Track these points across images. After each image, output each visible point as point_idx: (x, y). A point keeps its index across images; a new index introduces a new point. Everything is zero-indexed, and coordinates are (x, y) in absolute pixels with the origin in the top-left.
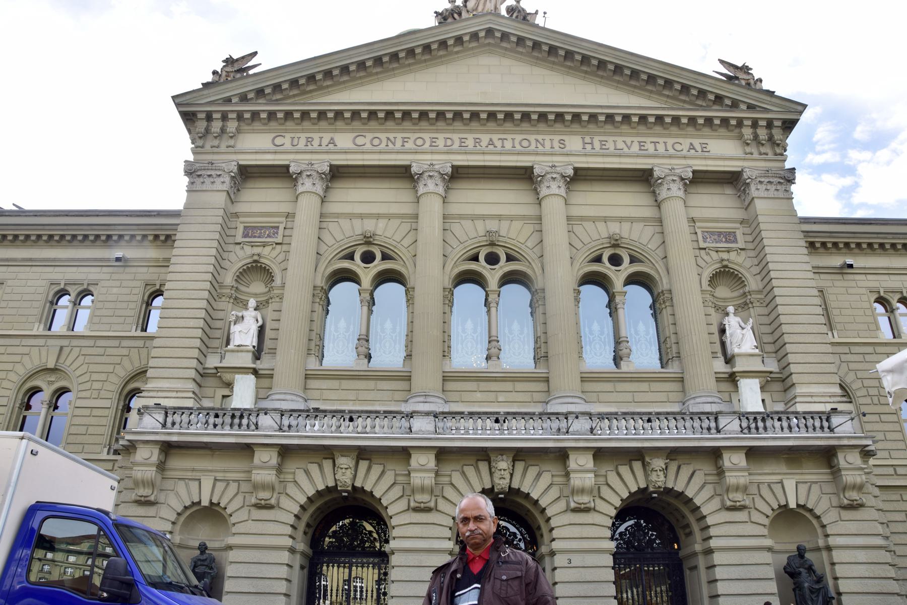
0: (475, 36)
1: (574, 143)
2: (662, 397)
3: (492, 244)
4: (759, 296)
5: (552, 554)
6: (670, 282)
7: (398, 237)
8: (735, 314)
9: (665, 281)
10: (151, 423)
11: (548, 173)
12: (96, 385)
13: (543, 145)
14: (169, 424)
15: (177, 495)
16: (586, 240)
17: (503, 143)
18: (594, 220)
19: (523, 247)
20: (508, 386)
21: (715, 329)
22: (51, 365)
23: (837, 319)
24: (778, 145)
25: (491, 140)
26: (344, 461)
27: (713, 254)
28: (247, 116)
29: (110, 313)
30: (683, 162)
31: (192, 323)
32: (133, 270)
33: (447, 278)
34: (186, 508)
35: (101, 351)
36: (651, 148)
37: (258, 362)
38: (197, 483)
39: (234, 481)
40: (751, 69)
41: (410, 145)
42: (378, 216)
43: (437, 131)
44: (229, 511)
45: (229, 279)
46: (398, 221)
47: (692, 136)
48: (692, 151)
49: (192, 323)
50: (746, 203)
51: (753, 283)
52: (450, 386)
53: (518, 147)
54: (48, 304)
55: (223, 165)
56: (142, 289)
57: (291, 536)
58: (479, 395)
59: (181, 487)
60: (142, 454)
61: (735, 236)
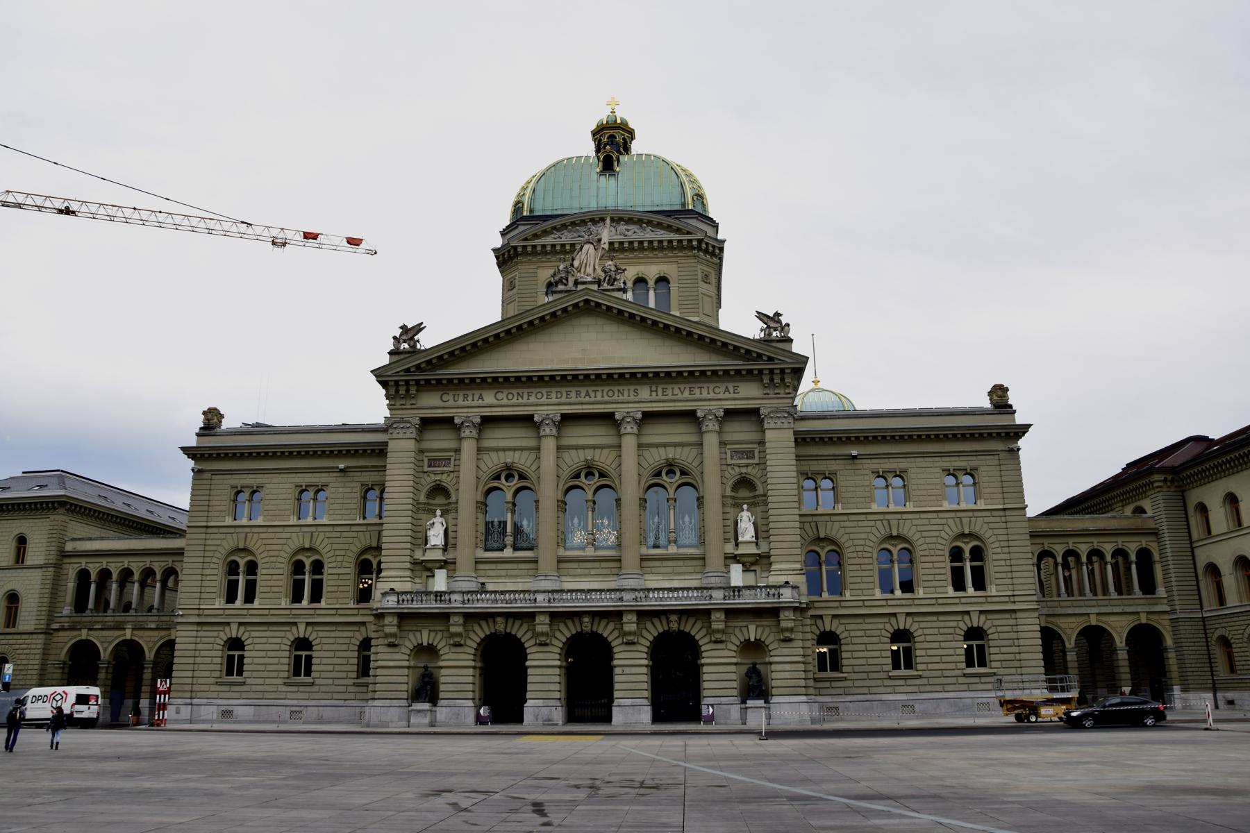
0: (576, 305)
1: (644, 392)
2: (690, 569)
3: (589, 467)
4: (764, 498)
5: (615, 666)
6: (703, 491)
7: (528, 464)
8: (747, 510)
9: (701, 489)
10: (391, 601)
11: (625, 417)
12: (339, 559)
13: (623, 394)
14: (401, 602)
15: (410, 640)
16: (651, 461)
17: (595, 394)
18: (657, 446)
19: (609, 468)
20: (597, 565)
21: (730, 523)
22: (307, 546)
23: (843, 495)
24: (788, 386)
25: (587, 391)
26: (499, 620)
27: (736, 468)
28: (422, 383)
29: (340, 506)
30: (719, 403)
31: (403, 533)
32: (351, 474)
33: (560, 492)
34: (415, 647)
35: (339, 534)
36: (697, 391)
37: (446, 553)
38: (419, 633)
39: (440, 631)
40: (780, 315)
41: (533, 399)
42: (514, 449)
43: (551, 387)
44: (438, 648)
45: (422, 498)
46: (527, 452)
47: (729, 381)
48: (727, 393)
49: (403, 533)
51: (760, 491)
52: (563, 565)
53: (606, 398)
54: (296, 501)
55: (410, 419)
56: (359, 488)
57: (474, 660)
58: (579, 570)
59: (411, 636)
60: (388, 620)
61: (754, 453)
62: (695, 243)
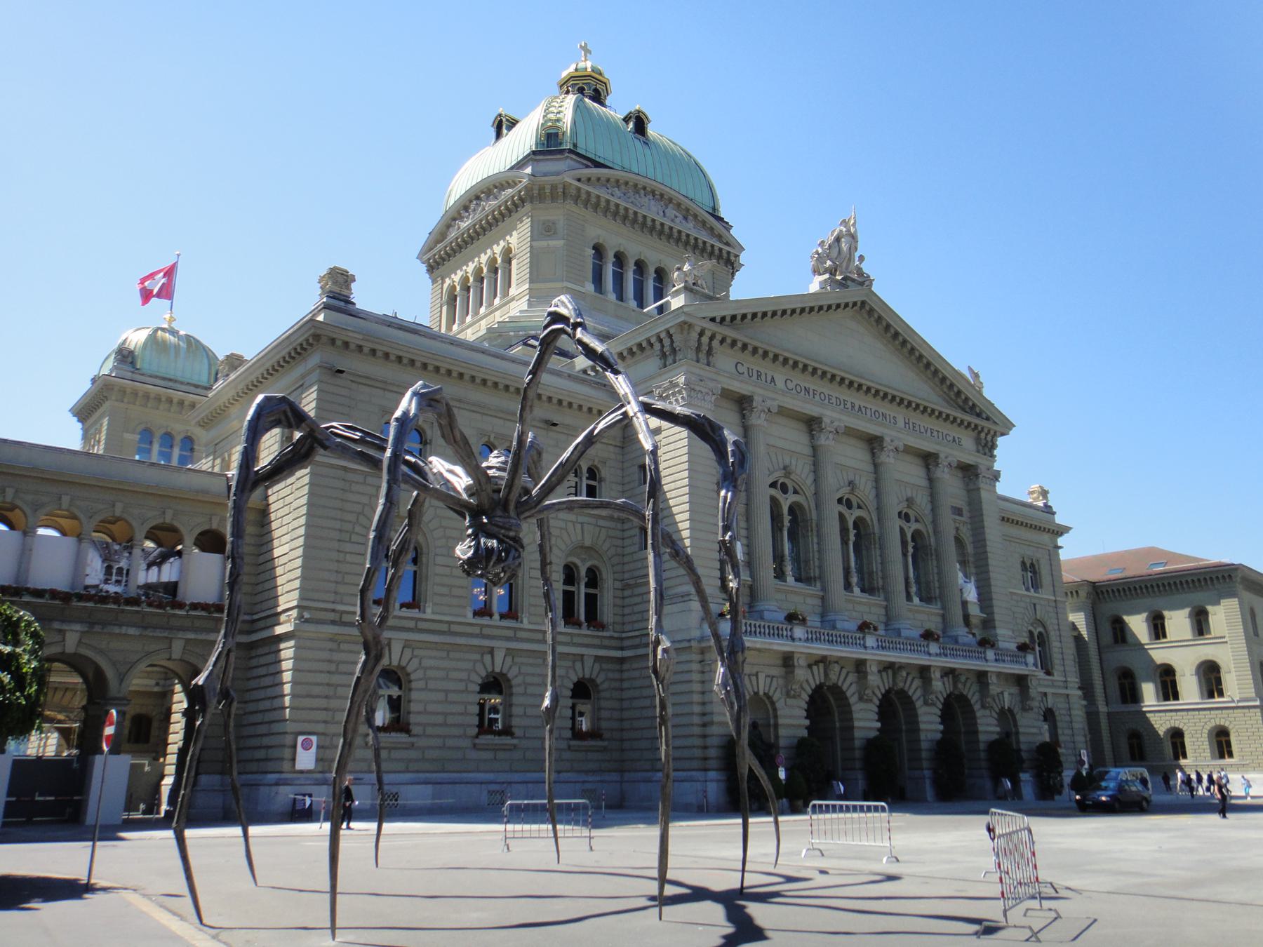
7: (803, 476)
36: (935, 434)
50: (972, 486)
62: (732, 258)
